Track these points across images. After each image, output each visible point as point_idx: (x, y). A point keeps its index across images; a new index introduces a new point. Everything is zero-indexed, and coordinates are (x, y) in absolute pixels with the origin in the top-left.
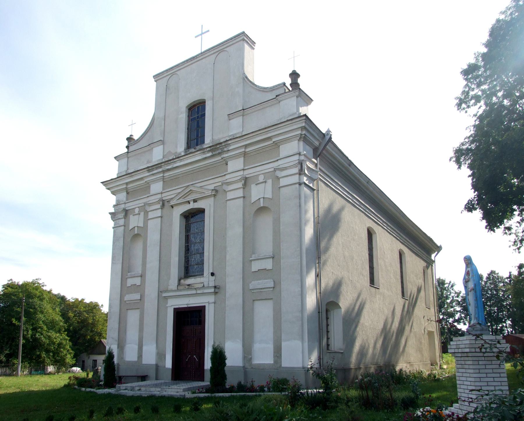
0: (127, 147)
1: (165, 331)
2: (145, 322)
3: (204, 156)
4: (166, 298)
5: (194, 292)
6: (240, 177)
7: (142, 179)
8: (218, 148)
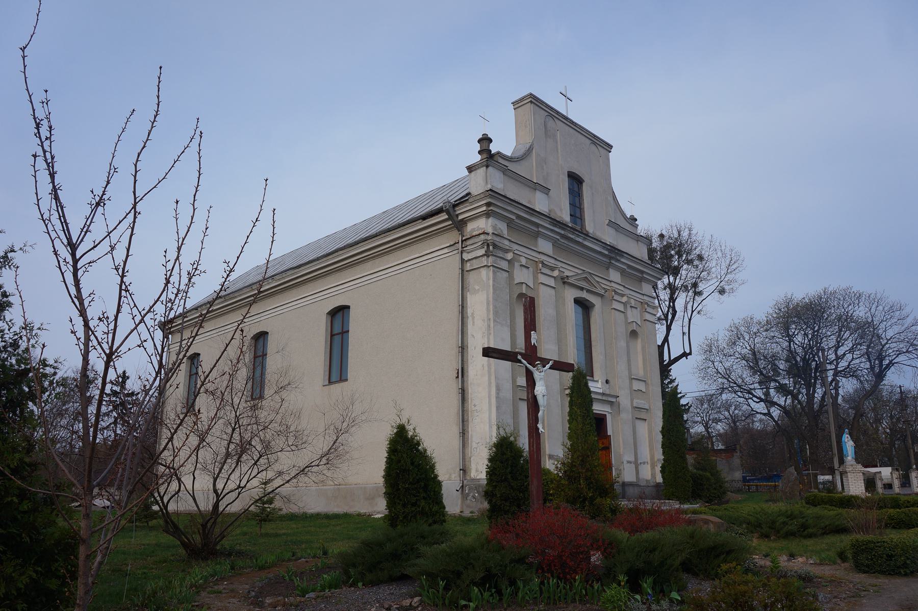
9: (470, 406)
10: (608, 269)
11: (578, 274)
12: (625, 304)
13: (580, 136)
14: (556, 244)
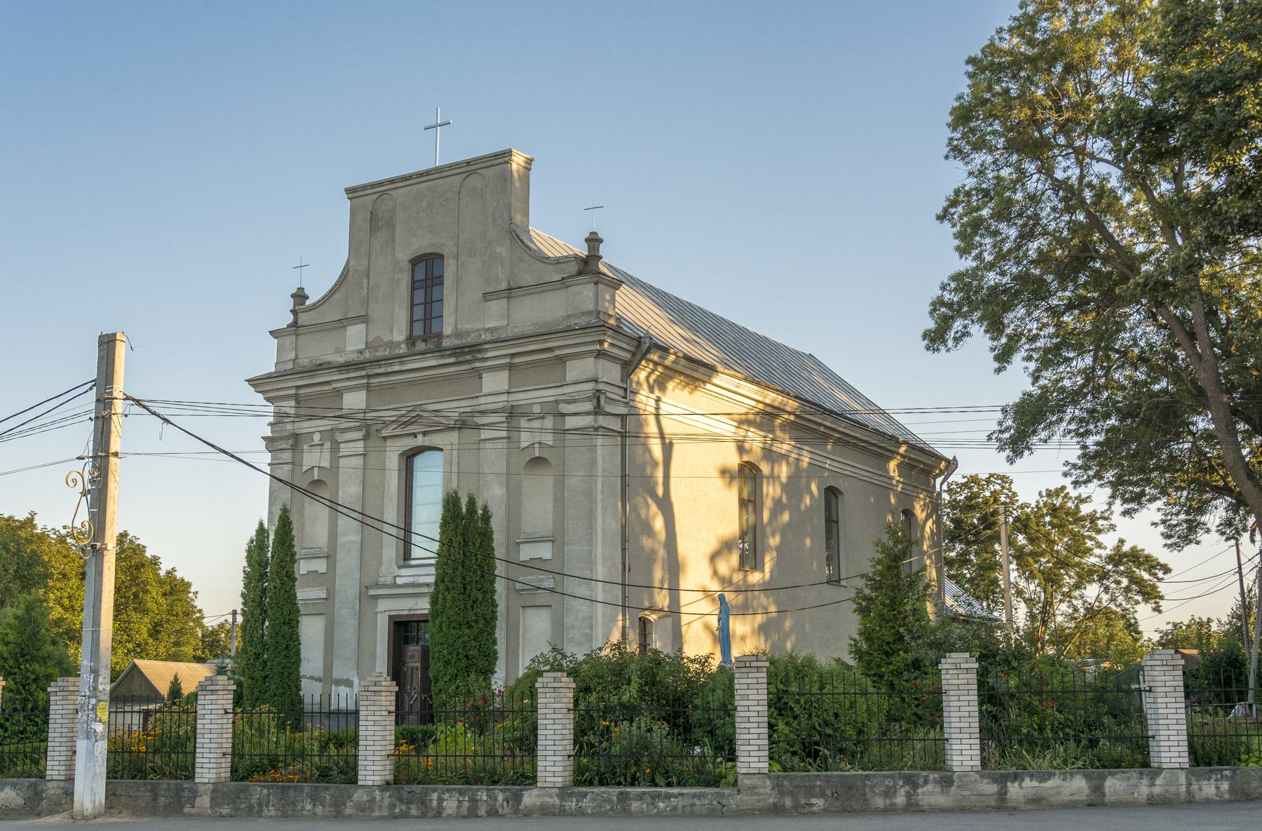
0: (294, 312)
1: (373, 656)
4: (375, 597)
6: (501, 405)
8: (468, 352)
13: (440, 182)
14: (368, 387)
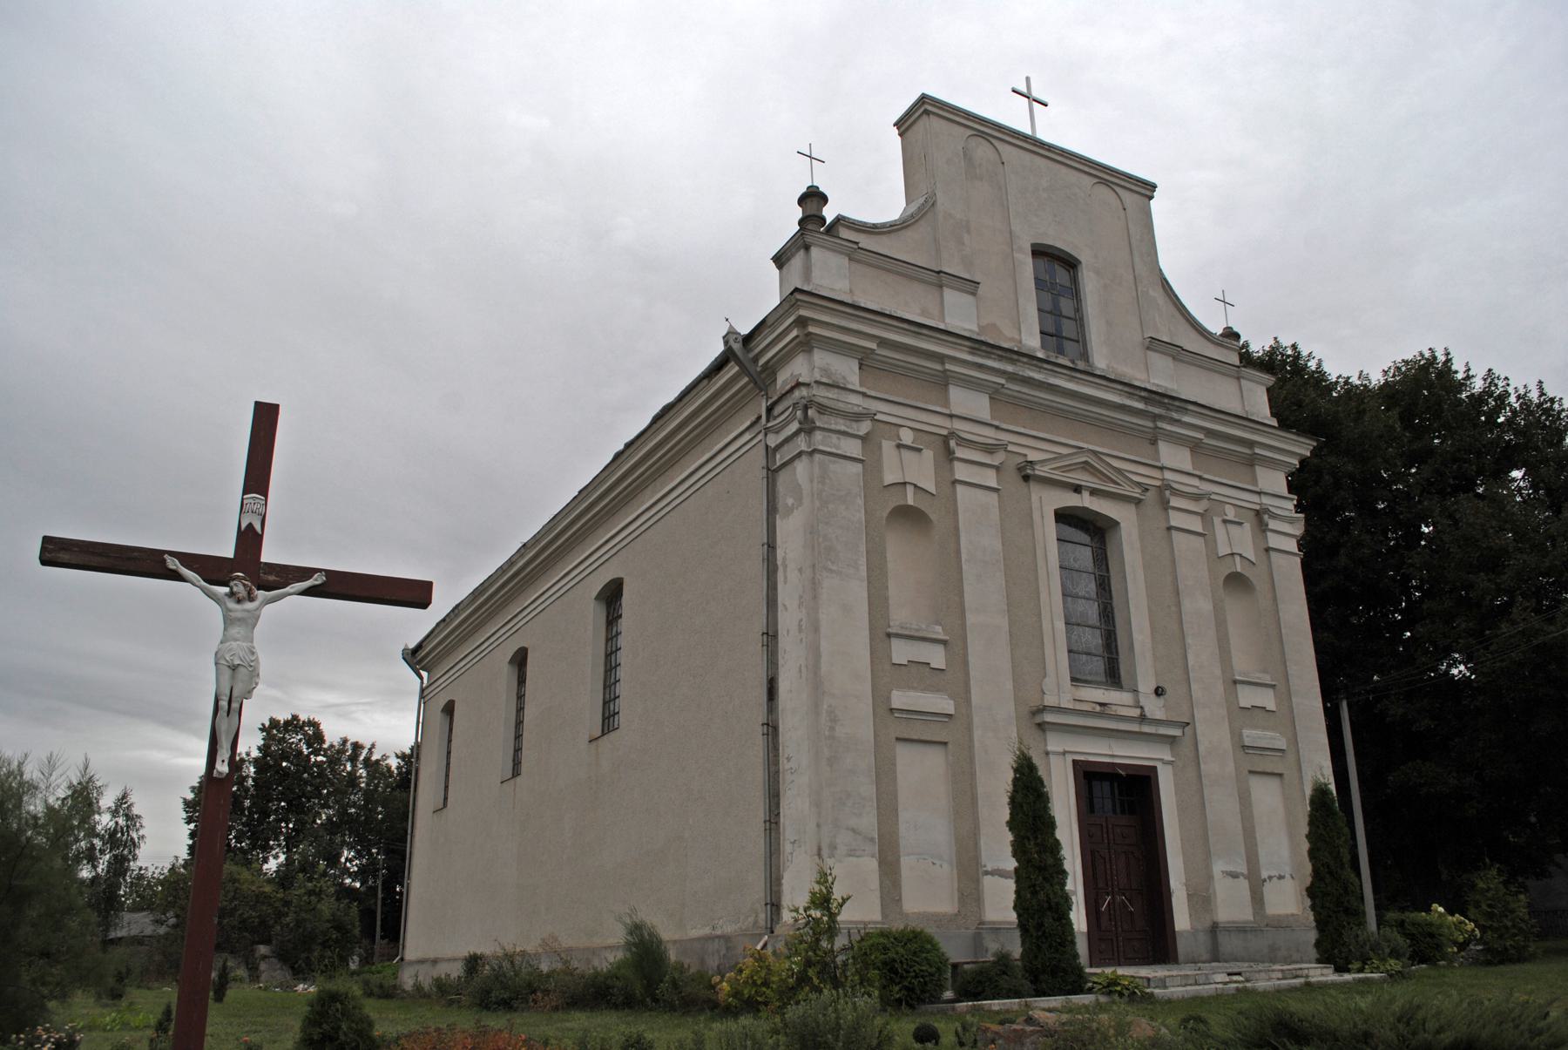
2: (980, 790)
3: (1128, 402)
5: (1135, 727)
7: (941, 358)
9: (784, 765)
10: (1154, 442)
11: (1061, 456)
12: (1204, 516)
13: (1064, 170)
14: (996, 395)
